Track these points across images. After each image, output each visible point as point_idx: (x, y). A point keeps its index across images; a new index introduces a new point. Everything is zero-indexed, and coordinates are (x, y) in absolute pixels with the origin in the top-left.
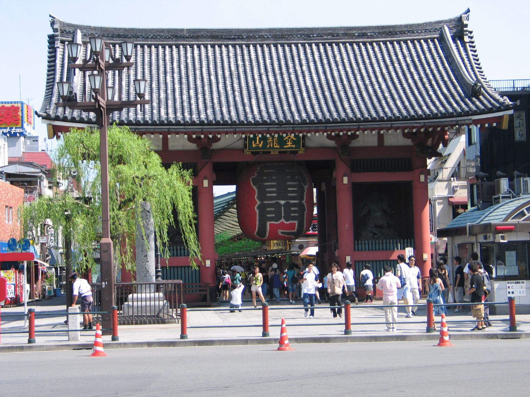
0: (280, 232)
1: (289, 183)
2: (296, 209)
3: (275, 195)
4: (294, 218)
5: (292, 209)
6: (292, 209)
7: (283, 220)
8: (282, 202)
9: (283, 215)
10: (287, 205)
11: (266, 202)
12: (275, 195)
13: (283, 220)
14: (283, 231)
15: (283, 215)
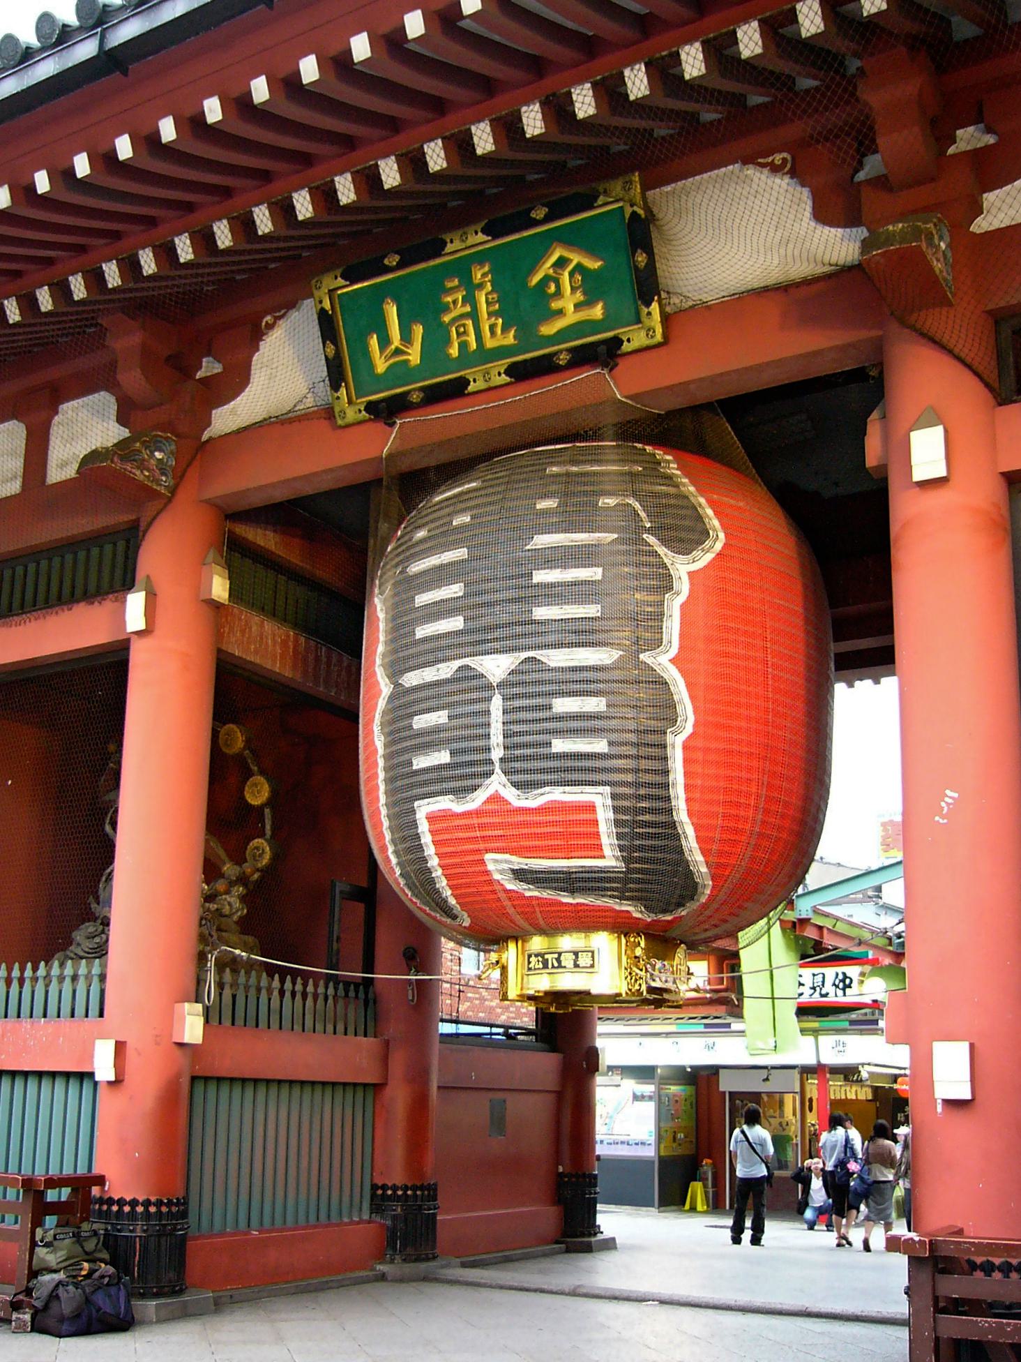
0: (499, 865)
1: (543, 540)
2: (595, 704)
3: (457, 623)
4: (577, 770)
5: (563, 705)
6: (563, 705)
7: (498, 784)
8: (496, 666)
9: (497, 754)
10: (529, 687)
11: (412, 679)
12: (457, 623)
13: (498, 784)
14: (519, 862)
15: (497, 754)
